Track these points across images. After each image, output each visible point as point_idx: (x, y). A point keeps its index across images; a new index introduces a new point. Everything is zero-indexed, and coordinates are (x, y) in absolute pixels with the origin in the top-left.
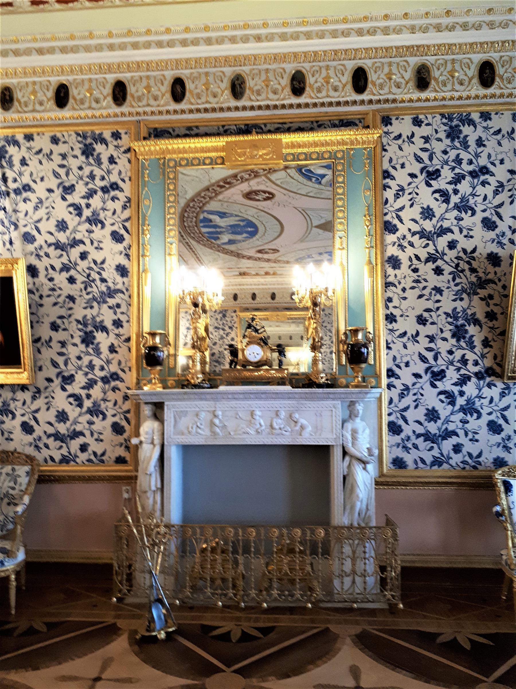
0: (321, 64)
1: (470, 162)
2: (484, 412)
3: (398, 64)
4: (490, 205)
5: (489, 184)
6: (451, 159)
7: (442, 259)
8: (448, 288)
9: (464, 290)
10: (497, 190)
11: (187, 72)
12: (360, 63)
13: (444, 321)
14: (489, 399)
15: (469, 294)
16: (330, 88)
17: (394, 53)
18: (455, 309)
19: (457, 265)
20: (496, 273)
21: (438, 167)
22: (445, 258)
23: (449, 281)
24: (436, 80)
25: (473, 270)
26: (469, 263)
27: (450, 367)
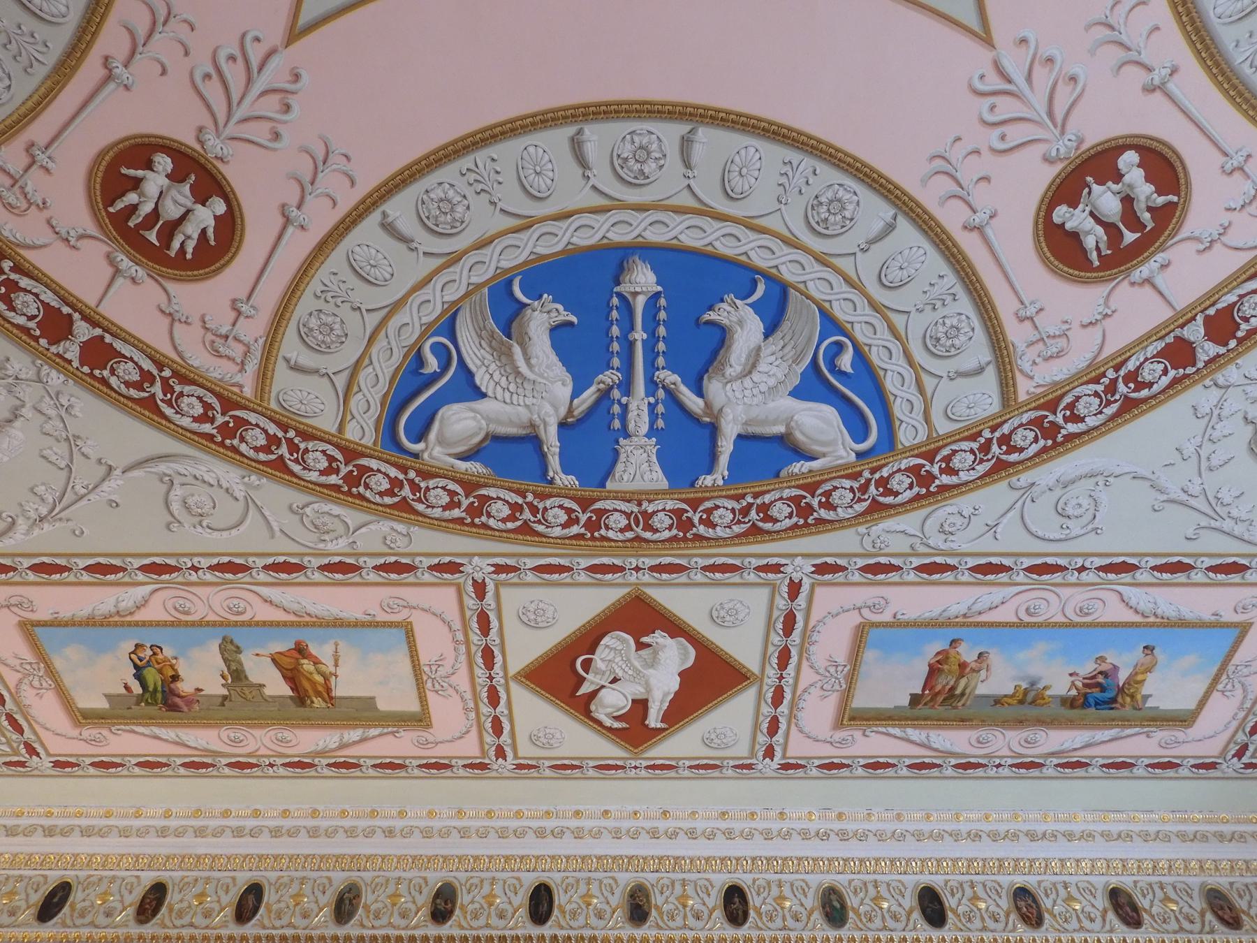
0: (483, 875)
3: (601, 882)
11: (273, 875)
12: (544, 877)
16: (493, 914)
17: (594, 865)
24: (657, 907)
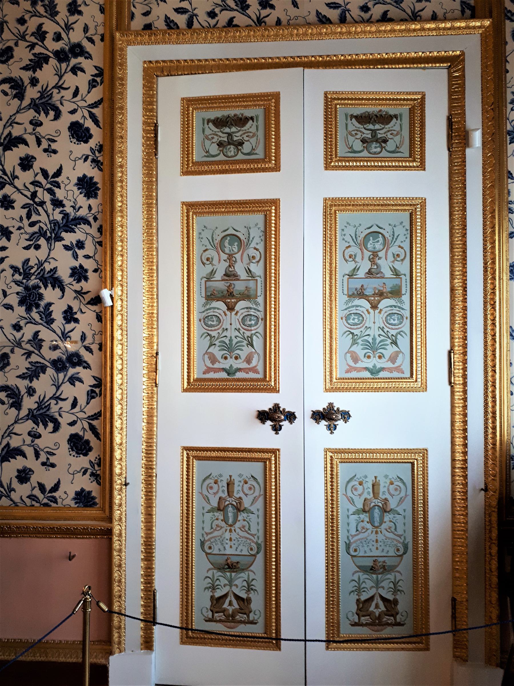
1: (58, 37)
2: (64, 421)
4: (82, 104)
5: (83, 71)
6: (29, 32)
7: (12, 184)
8: (19, 228)
9: (42, 233)
10: (94, 81)
13: (10, 279)
14: (70, 401)
15: (48, 240)
18: (28, 260)
19: (34, 195)
20: (90, 208)
21: (11, 44)
22: (16, 182)
23: (21, 219)
25: (57, 203)
26: (51, 192)
27: (16, 349)
